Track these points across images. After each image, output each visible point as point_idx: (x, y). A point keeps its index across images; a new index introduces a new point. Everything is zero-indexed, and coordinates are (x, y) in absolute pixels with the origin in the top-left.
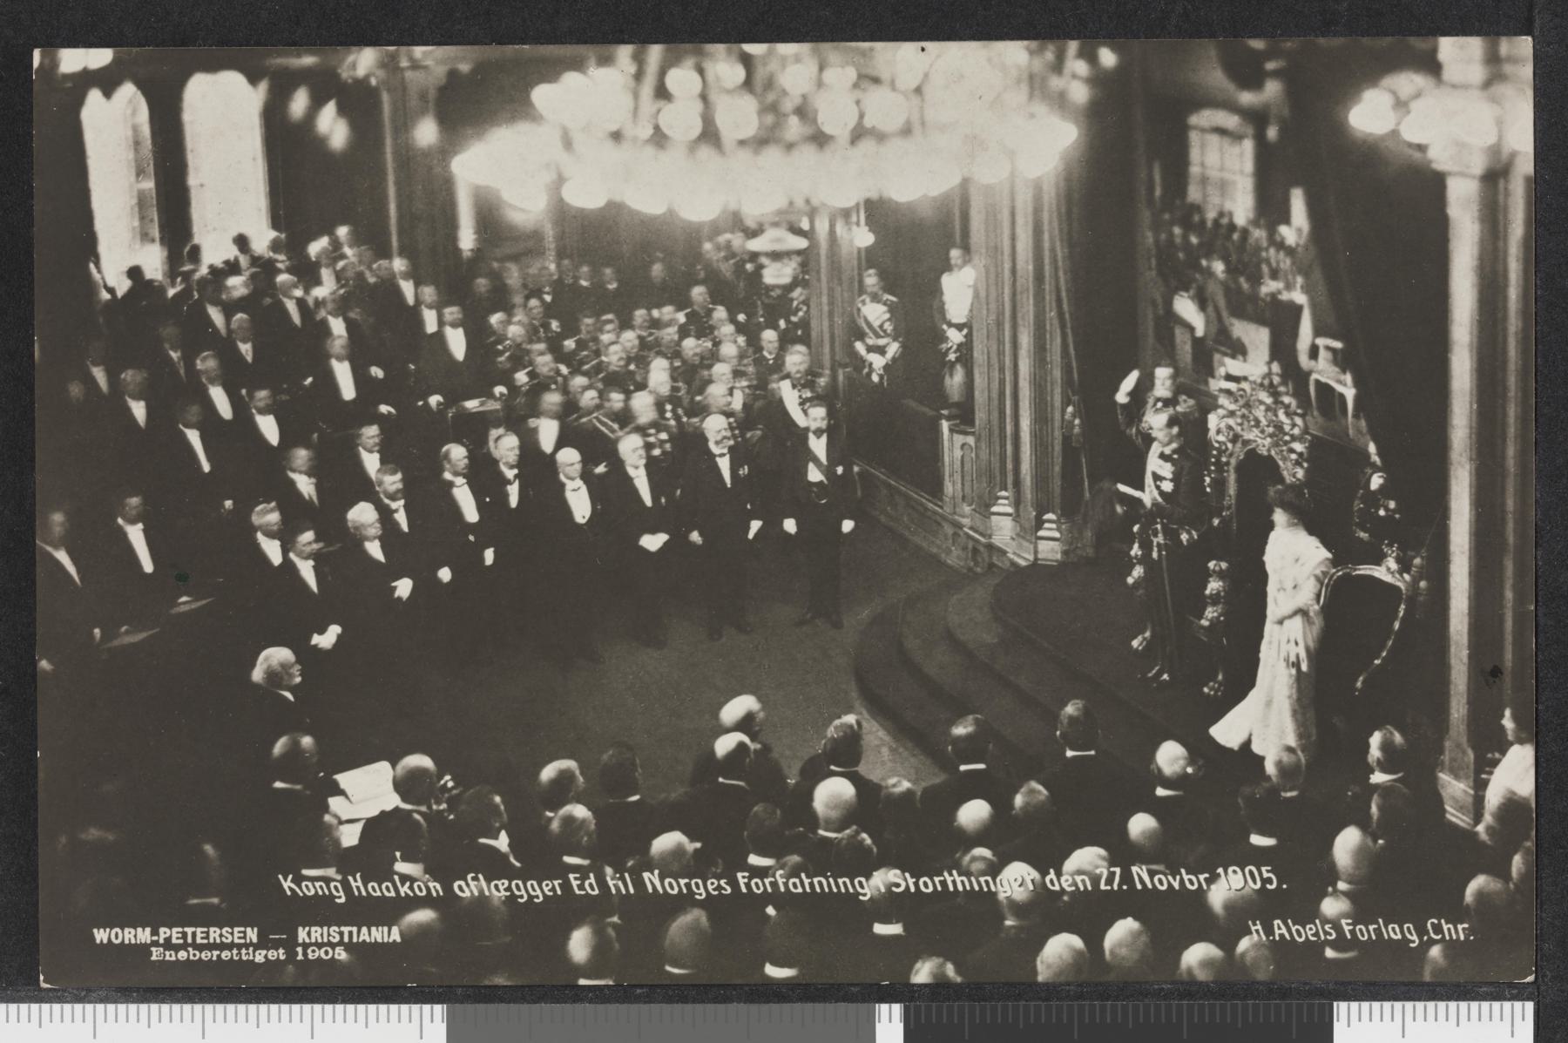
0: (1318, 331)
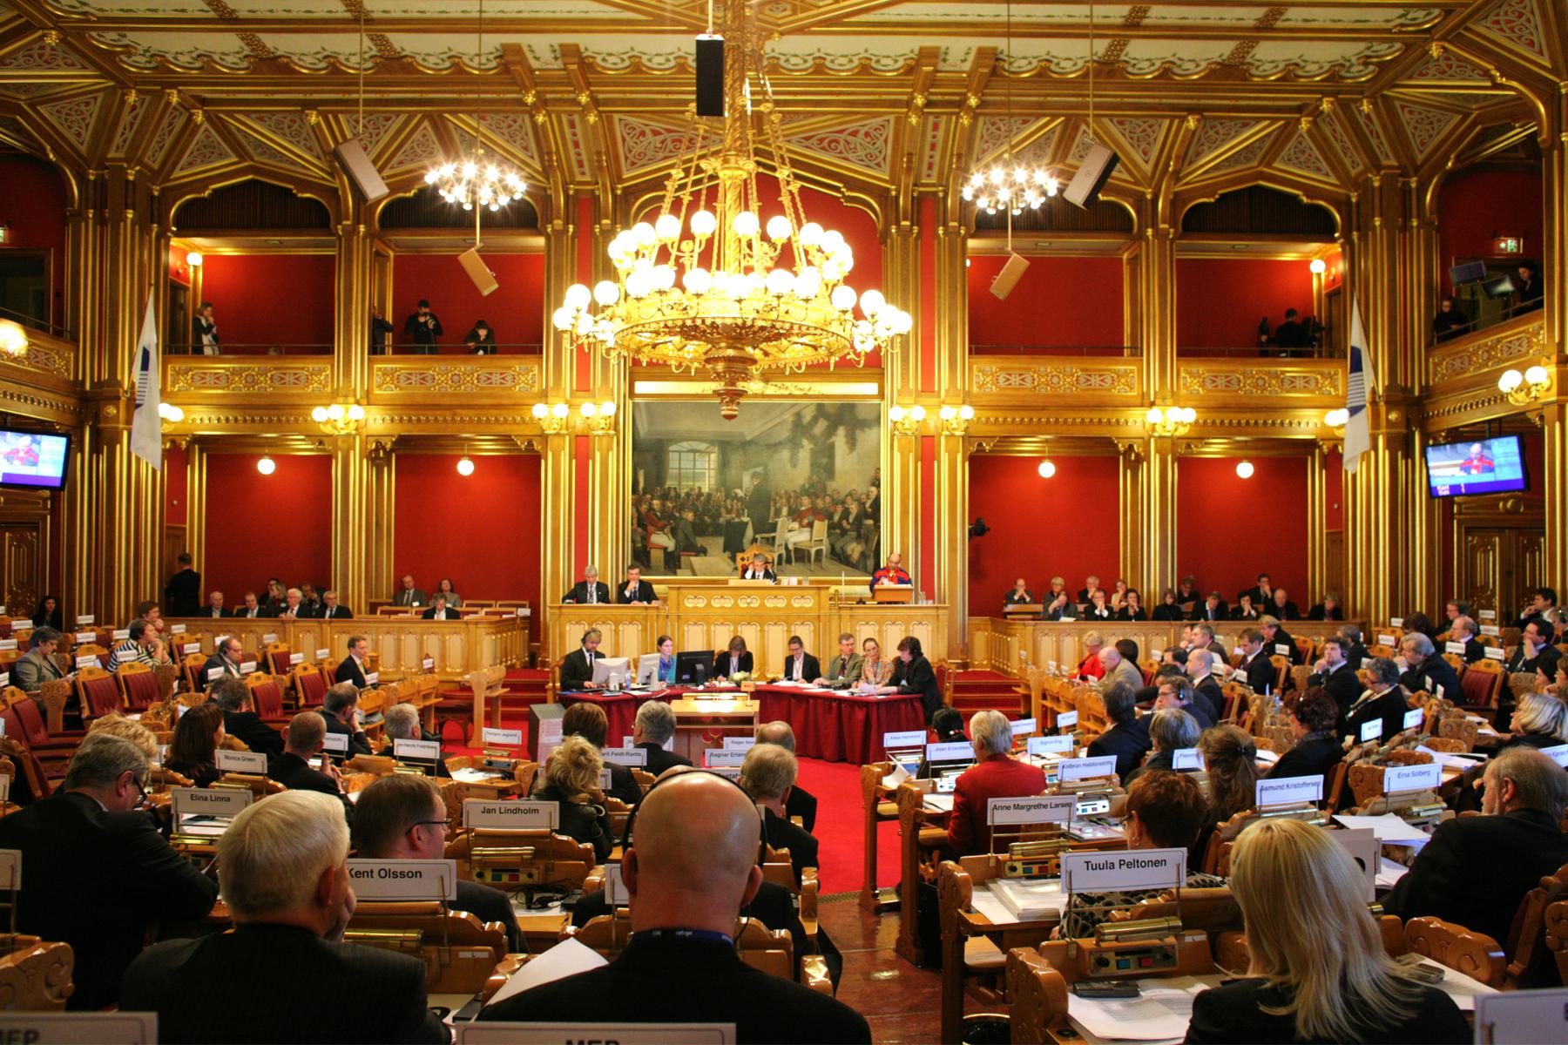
0: (756, 532)
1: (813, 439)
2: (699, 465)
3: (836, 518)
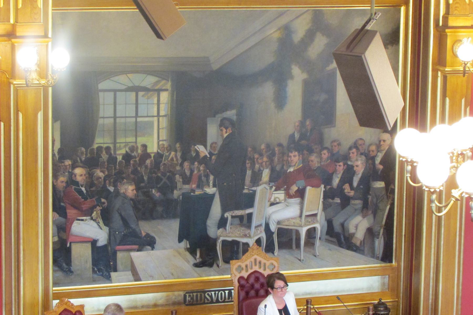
0: (225, 209)
1: (307, 66)
2: (142, 110)
3: (336, 181)
